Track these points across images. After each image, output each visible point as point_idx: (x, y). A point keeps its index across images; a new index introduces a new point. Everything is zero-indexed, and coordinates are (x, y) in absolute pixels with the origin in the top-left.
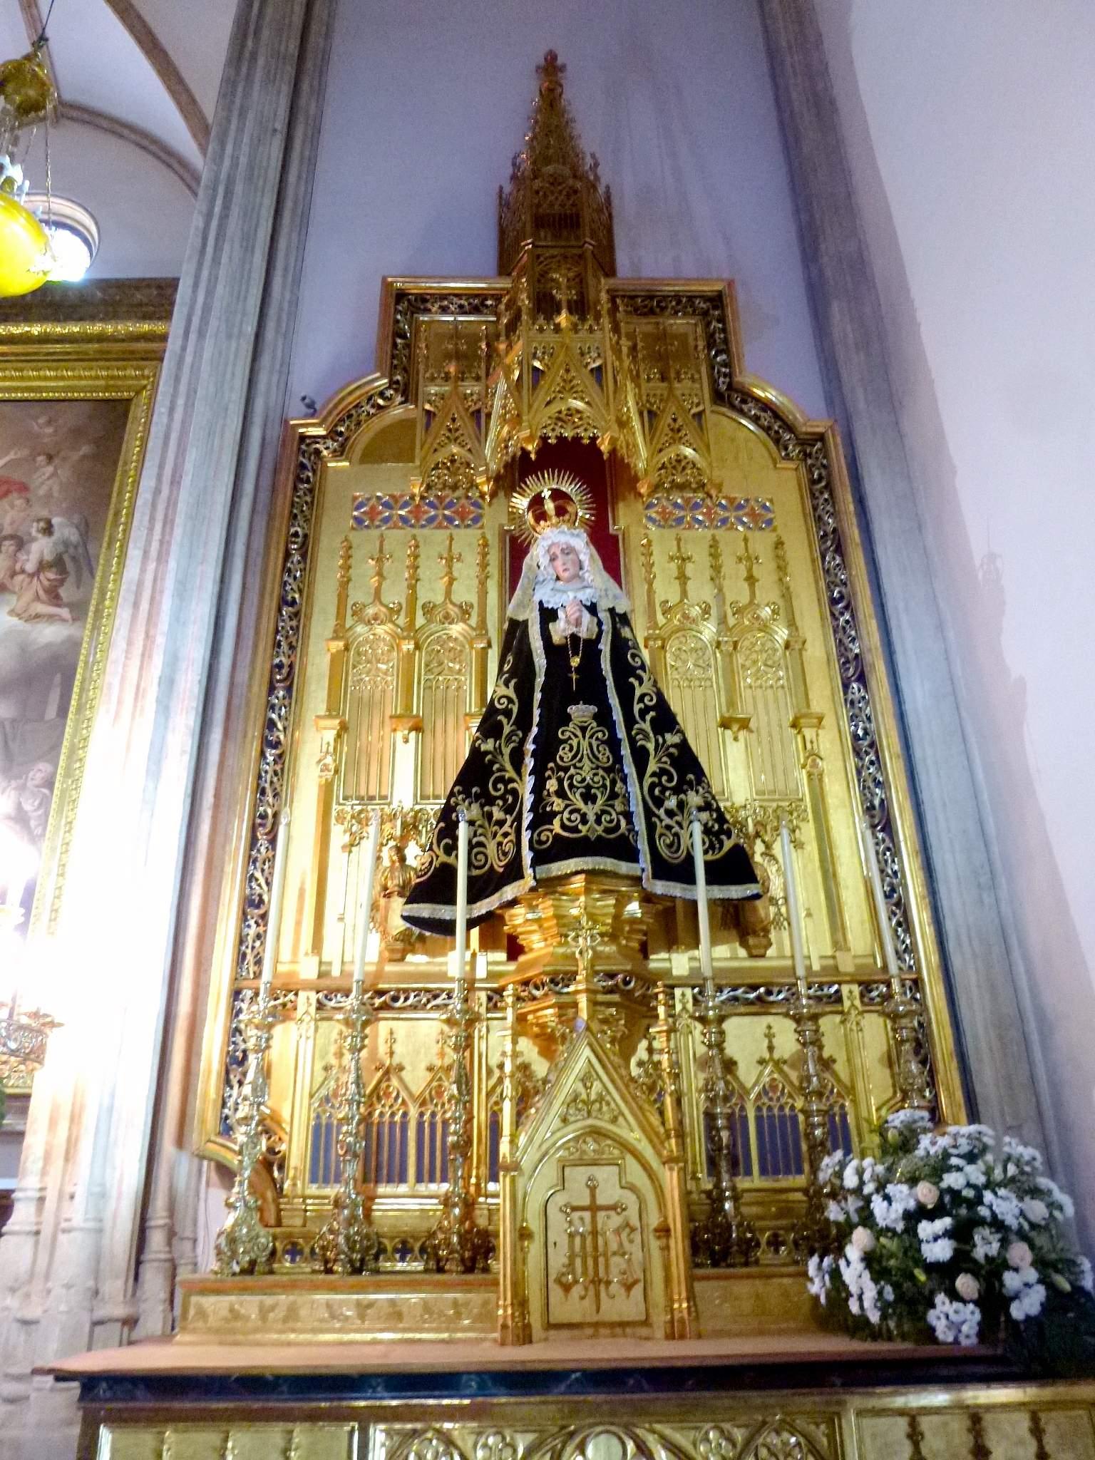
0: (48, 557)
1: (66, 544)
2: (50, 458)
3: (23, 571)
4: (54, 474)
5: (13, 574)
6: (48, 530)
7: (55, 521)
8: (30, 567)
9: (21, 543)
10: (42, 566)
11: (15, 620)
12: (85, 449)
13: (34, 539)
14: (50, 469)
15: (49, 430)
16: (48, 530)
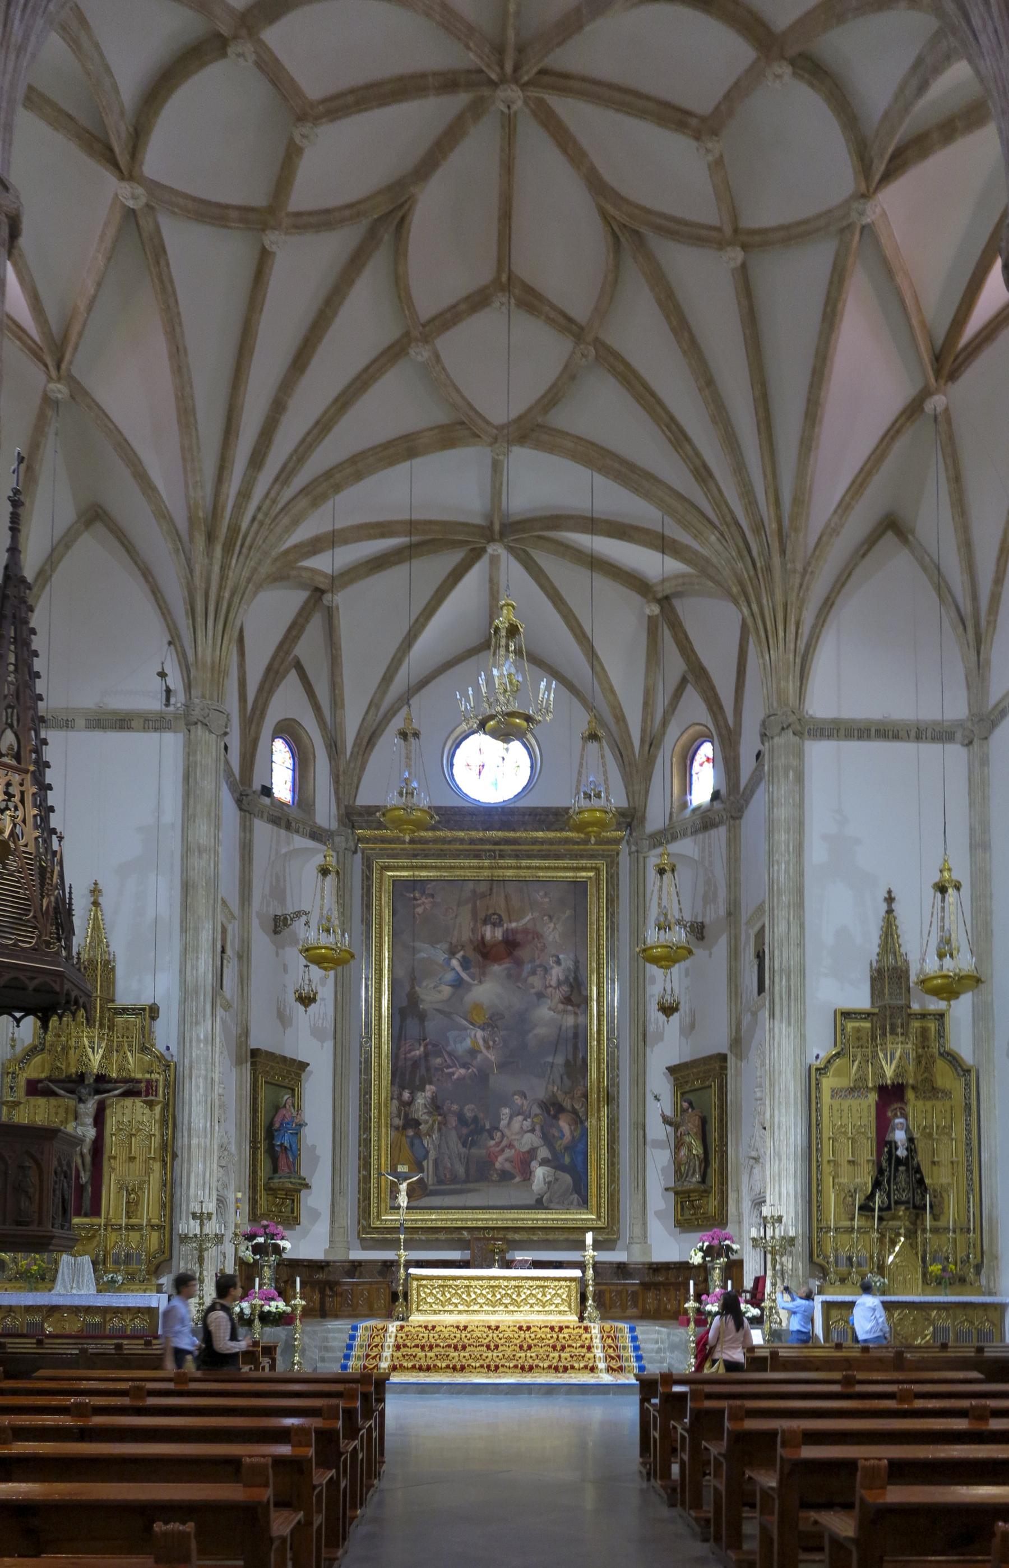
0: (562, 977)
1: (569, 969)
2: (551, 918)
3: (551, 986)
4: (555, 928)
5: (546, 987)
6: (558, 962)
7: (561, 956)
8: (554, 983)
9: (546, 970)
10: (559, 984)
11: (552, 1013)
12: (568, 912)
13: (552, 968)
14: (552, 925)
15: (547, 900)
16: (558, 962)
